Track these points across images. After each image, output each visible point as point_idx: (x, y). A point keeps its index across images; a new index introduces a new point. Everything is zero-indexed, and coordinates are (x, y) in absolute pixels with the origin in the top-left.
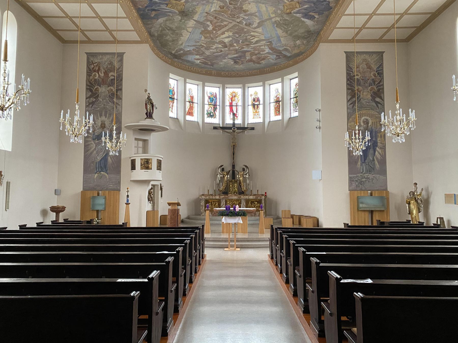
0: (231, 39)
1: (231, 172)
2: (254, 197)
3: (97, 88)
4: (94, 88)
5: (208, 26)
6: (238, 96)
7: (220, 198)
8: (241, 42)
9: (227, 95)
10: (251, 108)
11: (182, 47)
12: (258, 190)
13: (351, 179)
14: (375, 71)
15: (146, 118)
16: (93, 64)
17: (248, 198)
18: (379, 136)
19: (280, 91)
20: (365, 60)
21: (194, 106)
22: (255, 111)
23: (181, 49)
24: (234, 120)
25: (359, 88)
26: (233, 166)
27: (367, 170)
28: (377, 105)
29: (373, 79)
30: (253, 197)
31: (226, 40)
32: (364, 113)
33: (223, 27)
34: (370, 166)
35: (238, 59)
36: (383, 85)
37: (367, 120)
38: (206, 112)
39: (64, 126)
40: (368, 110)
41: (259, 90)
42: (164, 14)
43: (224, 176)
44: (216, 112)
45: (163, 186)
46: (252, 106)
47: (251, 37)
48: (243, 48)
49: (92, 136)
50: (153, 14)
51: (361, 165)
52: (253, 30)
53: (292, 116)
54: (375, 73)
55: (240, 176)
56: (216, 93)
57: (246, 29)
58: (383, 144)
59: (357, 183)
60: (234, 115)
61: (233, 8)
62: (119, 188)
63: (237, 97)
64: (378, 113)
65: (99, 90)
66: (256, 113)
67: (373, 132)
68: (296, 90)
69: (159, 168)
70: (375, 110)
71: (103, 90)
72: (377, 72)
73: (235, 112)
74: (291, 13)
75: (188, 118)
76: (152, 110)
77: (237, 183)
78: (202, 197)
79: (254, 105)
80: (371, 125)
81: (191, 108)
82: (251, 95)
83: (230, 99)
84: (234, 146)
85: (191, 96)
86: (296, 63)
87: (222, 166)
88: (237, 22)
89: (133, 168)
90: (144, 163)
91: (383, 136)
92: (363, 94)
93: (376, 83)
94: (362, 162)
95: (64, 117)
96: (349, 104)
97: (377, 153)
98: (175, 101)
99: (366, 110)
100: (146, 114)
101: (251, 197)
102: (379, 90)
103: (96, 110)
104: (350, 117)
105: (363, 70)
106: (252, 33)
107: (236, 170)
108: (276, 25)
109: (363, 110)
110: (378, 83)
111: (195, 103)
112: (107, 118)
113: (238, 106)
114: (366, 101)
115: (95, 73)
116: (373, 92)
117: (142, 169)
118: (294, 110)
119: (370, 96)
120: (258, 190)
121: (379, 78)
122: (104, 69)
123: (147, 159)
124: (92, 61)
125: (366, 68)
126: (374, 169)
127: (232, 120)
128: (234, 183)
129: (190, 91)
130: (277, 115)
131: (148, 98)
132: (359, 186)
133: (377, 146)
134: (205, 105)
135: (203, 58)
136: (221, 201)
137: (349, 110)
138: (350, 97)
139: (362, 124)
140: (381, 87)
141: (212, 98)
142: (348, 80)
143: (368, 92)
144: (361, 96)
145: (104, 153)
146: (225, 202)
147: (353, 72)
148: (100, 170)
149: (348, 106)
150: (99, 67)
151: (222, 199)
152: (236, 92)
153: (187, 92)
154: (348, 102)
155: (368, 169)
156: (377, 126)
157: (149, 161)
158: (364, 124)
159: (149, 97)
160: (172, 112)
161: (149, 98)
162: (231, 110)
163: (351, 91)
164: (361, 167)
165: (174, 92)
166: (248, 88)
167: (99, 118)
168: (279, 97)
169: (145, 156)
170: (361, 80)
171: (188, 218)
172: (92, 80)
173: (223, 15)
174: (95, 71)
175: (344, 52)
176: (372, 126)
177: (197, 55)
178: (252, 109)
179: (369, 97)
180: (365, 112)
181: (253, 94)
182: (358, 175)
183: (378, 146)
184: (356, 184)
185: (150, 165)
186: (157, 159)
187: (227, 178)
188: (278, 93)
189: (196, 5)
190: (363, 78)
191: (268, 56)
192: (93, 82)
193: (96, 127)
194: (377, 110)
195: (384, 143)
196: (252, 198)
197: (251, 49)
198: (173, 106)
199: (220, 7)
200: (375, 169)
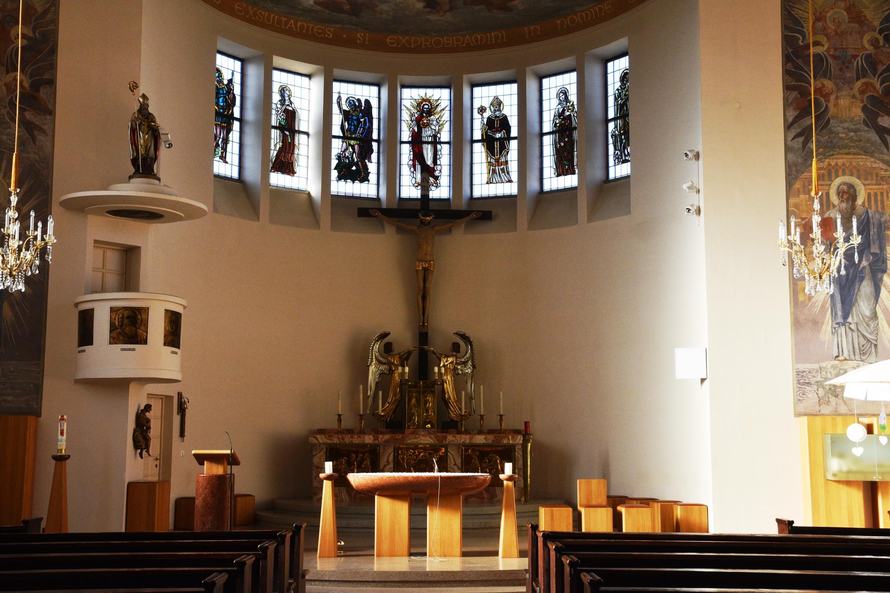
2: (491, 438)
6: (441, 111)
7: (377, 442)
9: (403, 108)
10: (479, 149)
13: (803, 376)
14: (875, 31)
17: (468, 441)
19: (573, 98)
21: (296, 143)
22: (493, 161)
24: (425, 186)
25: (823, 86)
26: (423, 337)
27: (854, 348)
28: (881, 138)
29: (868, 57)
30: (485, 439)
32: (840, 164)
37: (851, 186)
38: (334, 162)
40: (854, 154)
41: (508, 94)
43: (390, 369)
44: (370, 161)
45: (186, 401)
46: (485, 144)
51: (834, 331)
53: (612, 176)
54: (878, 36)
55: (443, 370)
56: (367, 102)
59: (821, 392)
60: (428, 174)
62: (35, 406)
63: (437, 116)
64: (885, 163)
66: (497, 168)
67: (872, 227)
68: (623, 96)
69: (173, 338)
70: (876, 155)
72: (883, 35)
73: (429, 162)
75: (278, 179)
77: (433, 392)
78: (318, 437)
79: (488, 141)
80: (864, 203)
82: (482, 110)
84: (425, 270)
85: (286, 111)
87: (384, 336)
89: (86, 337)
90: (122, 322)
92: (836, 105)
94: (836, 324)
96: (791, 135)
98: (236, 125)
99: (848, 154)
100: (134, 161)
101: (480, 439)
104: (796, 178)
105: (838, 27)
107: (432, 349)
109: (839, 154)
110: (885, 69)
111: (300, 132)
113: (441, 143)
114: (846, 125)
116: (871, 97)
117: (113, 340)
118: (618, 158)
119: (860, 111)
125: (847, 21)
126: (876, 346)
127: (419, 187)
128: (424, 393)
129: (282, 96)
130: (563, 172)
131: (139, 111)
132: (829, 401)
134: (334, 141)
136: (382, 450)
137: (791, 156)
138: (796, 113)
139: (834, 199)
141: (354, 118)
142: (787, 59)
143: (854, 97)
144: (832, 110)
146: (392, 454)
147: (804, 32)
149: (789, 143)
153: (276, 98)
154: (788, 129)
155: (856, 346)
157: (139, 317)
158: (842, 201)
159: (143, 109)
160: (226, 162)
162: (418, 157)
163: (799, 93)
164: (833, 340)
165: (231, 95)
166: (473, 85)
168: (570, 115)
170: (829, 58)
176: (866, 205)
178: (484, 155)
179: (857, 112)
180: (845, 160)
181: (486, 104)
182: (824, 364)
185: (142, 328)
186: (167, 311)
188: (568, 104)
194: (883, 154)
198: (226, 141)
200: (878, 346)
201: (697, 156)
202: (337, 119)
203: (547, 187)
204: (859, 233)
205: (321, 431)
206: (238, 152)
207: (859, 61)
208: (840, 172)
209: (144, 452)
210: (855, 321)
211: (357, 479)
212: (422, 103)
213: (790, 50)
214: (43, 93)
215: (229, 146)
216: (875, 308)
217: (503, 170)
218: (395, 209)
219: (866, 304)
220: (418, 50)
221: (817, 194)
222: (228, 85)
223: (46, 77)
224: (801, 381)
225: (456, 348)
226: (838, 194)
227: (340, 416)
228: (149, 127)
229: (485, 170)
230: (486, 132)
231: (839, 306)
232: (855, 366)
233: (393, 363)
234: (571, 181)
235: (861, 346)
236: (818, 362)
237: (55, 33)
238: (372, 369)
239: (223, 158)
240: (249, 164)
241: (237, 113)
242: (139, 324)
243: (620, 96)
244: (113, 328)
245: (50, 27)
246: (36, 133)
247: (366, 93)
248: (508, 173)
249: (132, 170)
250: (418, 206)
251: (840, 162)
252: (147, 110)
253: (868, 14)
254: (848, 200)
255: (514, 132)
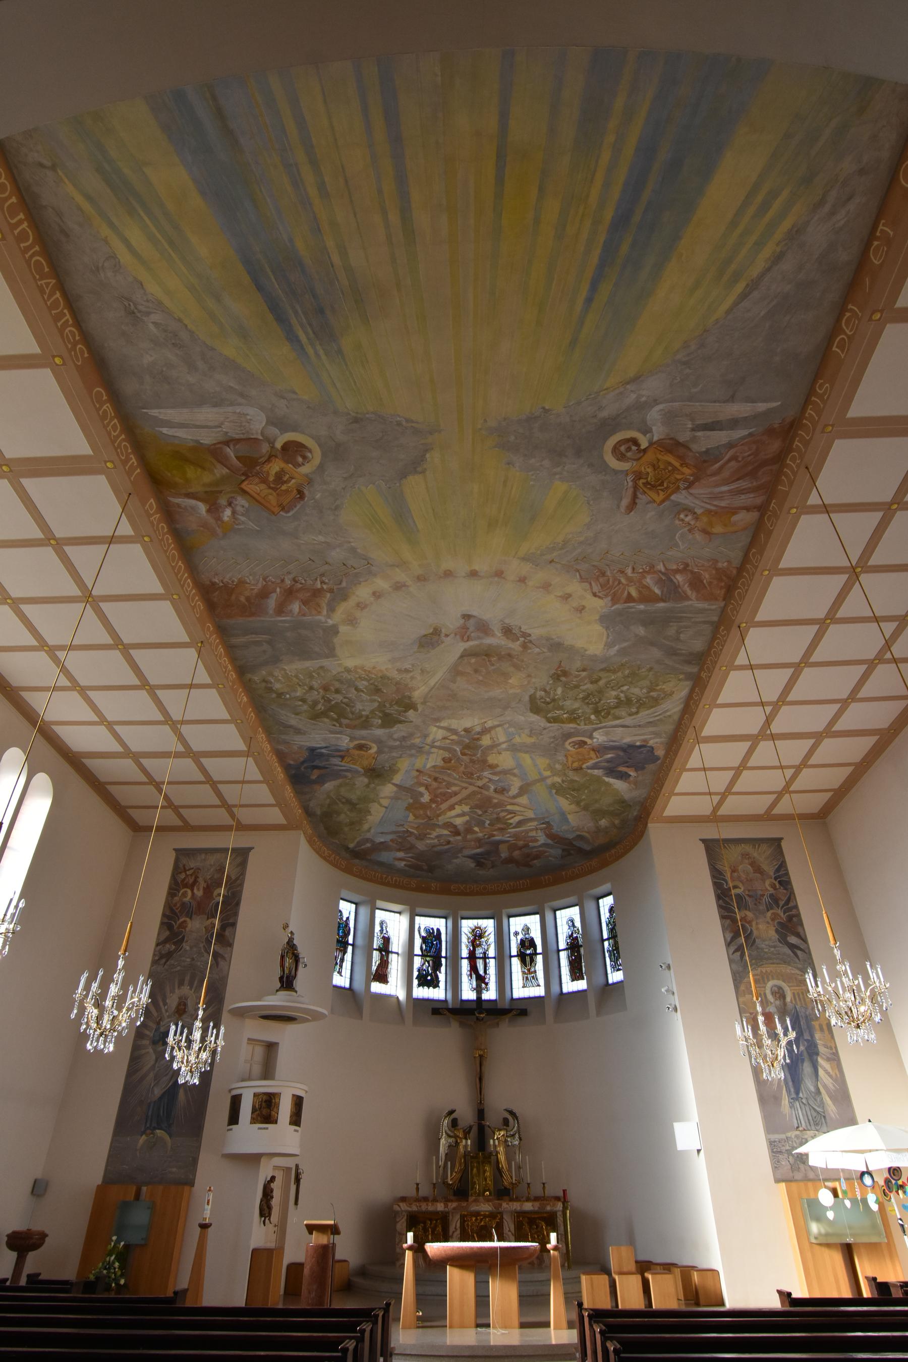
0: (467, 818)
1: (475, 1130)
2: (537, 1204)
3: (185, 921)
4: (178, 923)
5: (422, 795)
6: (488, 935)
7: (446, 1209)
8: (489, 825)
9: (463, 933)
10: (516, 963)
11: (368, 835)
12: (544, 1184)
15: (280, 988)
16: (185, 871)
17: (519, 1208)
18: (817, 1027)
19: (578, 924)
20: (747, 855)
21: (390, 961)
23: (367, 840)
24: (479, 990)
25: (746, 915)
26: (481, 1114)
27: (809, 1120)
29: (771, 896)
31: (459, 821)
33: (451, 797)
34: (813, 1108)
35: (485, 859)
36: (796, 907)
37: (780, 988)
38: (416, 974)
39: (82, 1009)
40: (777, 964)
41: (533, 922)
42: (336, 775)
43: (456, 1141)
44: (440, 972)
45: (302, 1172)
47: (508, 815)
48: (494, 836)
49: (152, 1035)
50: (314, 775)
51: (792, 1106)
52: (509, 800)
53: (610, 981)
55: (497, 1142)
56: (438, 930)
57: (495, 798)
58: (831, 1048)
59: (791, 1159)
60: (481, 981)
61: (468, 761)
62: (191, 1177)
65: (186, 927)
66: (529, 977)
67: (801, 1019)
69: (296, 1119)
71: (195, 925)
72: (777, 880)
73: (481, 972)
74: (581, 768)
75: (376, 987)
76: (294, 969)
77: (490, 1162)
78: (401, 1204)
79: (522, 956)
80: (791, 1000)
81: (384, 963)
82: (516, 934)
83: (471, 944)
84: (481, 1056)
85: (384, 938)
86: (604, 864)
87: (451, 1112)
88: (479, 787)
89: (234, 1119)
90: (261, 1105)
91: (825, 1027)
92: (757, 929)
93: (781, 903)
94: (792, 1099)
95: (87, 988)
96: (731, 951)
97: (821, 1072)
98: (350, 948)
99: (773, 963)
100: (281, 979)
101: (528, 1206)
102: (790, 919)
103: (172, 970)
106: (509, 807)
107: (488, 1124)
108: (554, 791)
109: (766, 964)
111: (392, 952)
112: (193, 990)
113: (489, 958)
114: (767, 943)
115: (185, 889)
116: (779, 923)
117: (254, 1121)
118: (613, 968)
120: (544, 1184)
121: (785, 891)
122: (205, 882)
123: (271, 1093)
124: (184, 866)
125: (752, 871)
126: (824, 1117)
127: (475, 991)
128: (483, 1163)
129: (382, 927)
131: (288, 943)
132: (799, 1168)
133: (817, 1054)
134: (416, 958)
135: (412, 857)
136: (451, 1217)
138: (732, 935)
139: (770, 998)
140: (794, 912)
141: (430, 941)
142: (718, 897)
143: (768, 923)
144: (755, 933)
145: (172, 1077)
146: (459, 1222)
148: (154, 1125)
149: (731, 956)
150: (196, 877)
151: (452, 1213)
152: (483, 926)
153: (377, 928)
155: (810, 1118)
156: (806, 1004)
157: (274, 1101)
158: (776, 999)
160: (341, 976)
161: (291, 943)
162: (473, 968)
163: (731, 921)
166: (509, 917)
167: (176, 991)
168: (577, 937)
169: (266, 1086)
170: (746, 896)
171: (362, 1272)
172: (175, 905)
173: (449, 775)
174: (186, 886)
175: (701, 840)
176: (794, 1002)
177: (399, 850)
178: (519, 966)
179: (772, 933)
181: (519, 930)
182: (789, 1134)
183: (820, 1054)
184: (789, 1161)
186: (294, 1095)
187: (466, 1146)
189: (398, 758)
190: (750, 893)
191: (546, 852)
192: (177, 909)
193: (167, 1011)
194: (796, 963)
195: (833, 1046)
196: (532, 1208)
197: (509, 837)
198: (342, 960)
199: (444, 759)
200: (827, 1117)
201: (669, 967)
202: (418, 942)
203: (565, 990)
204: (793, 1029)
205: (403, 1199)
206: (350, 968)
207: (766, 899)
208: (770, 977)
209: (267, 1220)
210: (805, 1096)
211: (433, 1248)
212: (475, 929)
213: (719, 892)
214: (227, 933)
215: (344, 964)
216: (817, 1085)
217: (533, 977)
218: (458, 1009)
219: (810, 1082)
220: (471, 893)
221: (757, 999)
222: (346, 920)
223: (231, 921)
224: (775, 1150)
225: (506, 1122)
226: (772, 993)
227: (418, 1184)
228: (293, 954)
229: (521, 978)
230: (520, 950)
231: (790, 1084)
232: (813, 1135)
233: (458, 1137)
234: (582, 985)
235: (814, 1117)
236: (784, 1133)
237: (241, 892)
238: (443, 1141)
239: (340, 973)
240: (357, 977)
241: (351, 940)
242: (273, 1107)
243: (610, 922)
244: (254, 1110)
245: (238, 889)
246: (219, 959)
247: (438, 924)
248: (537, 979)
249: (279, 985)
250: (474, 1006)
251: (768, 969)
252: (293, 942)
253: (765, 867)
254: (779, 998)
255: (539, 950)
